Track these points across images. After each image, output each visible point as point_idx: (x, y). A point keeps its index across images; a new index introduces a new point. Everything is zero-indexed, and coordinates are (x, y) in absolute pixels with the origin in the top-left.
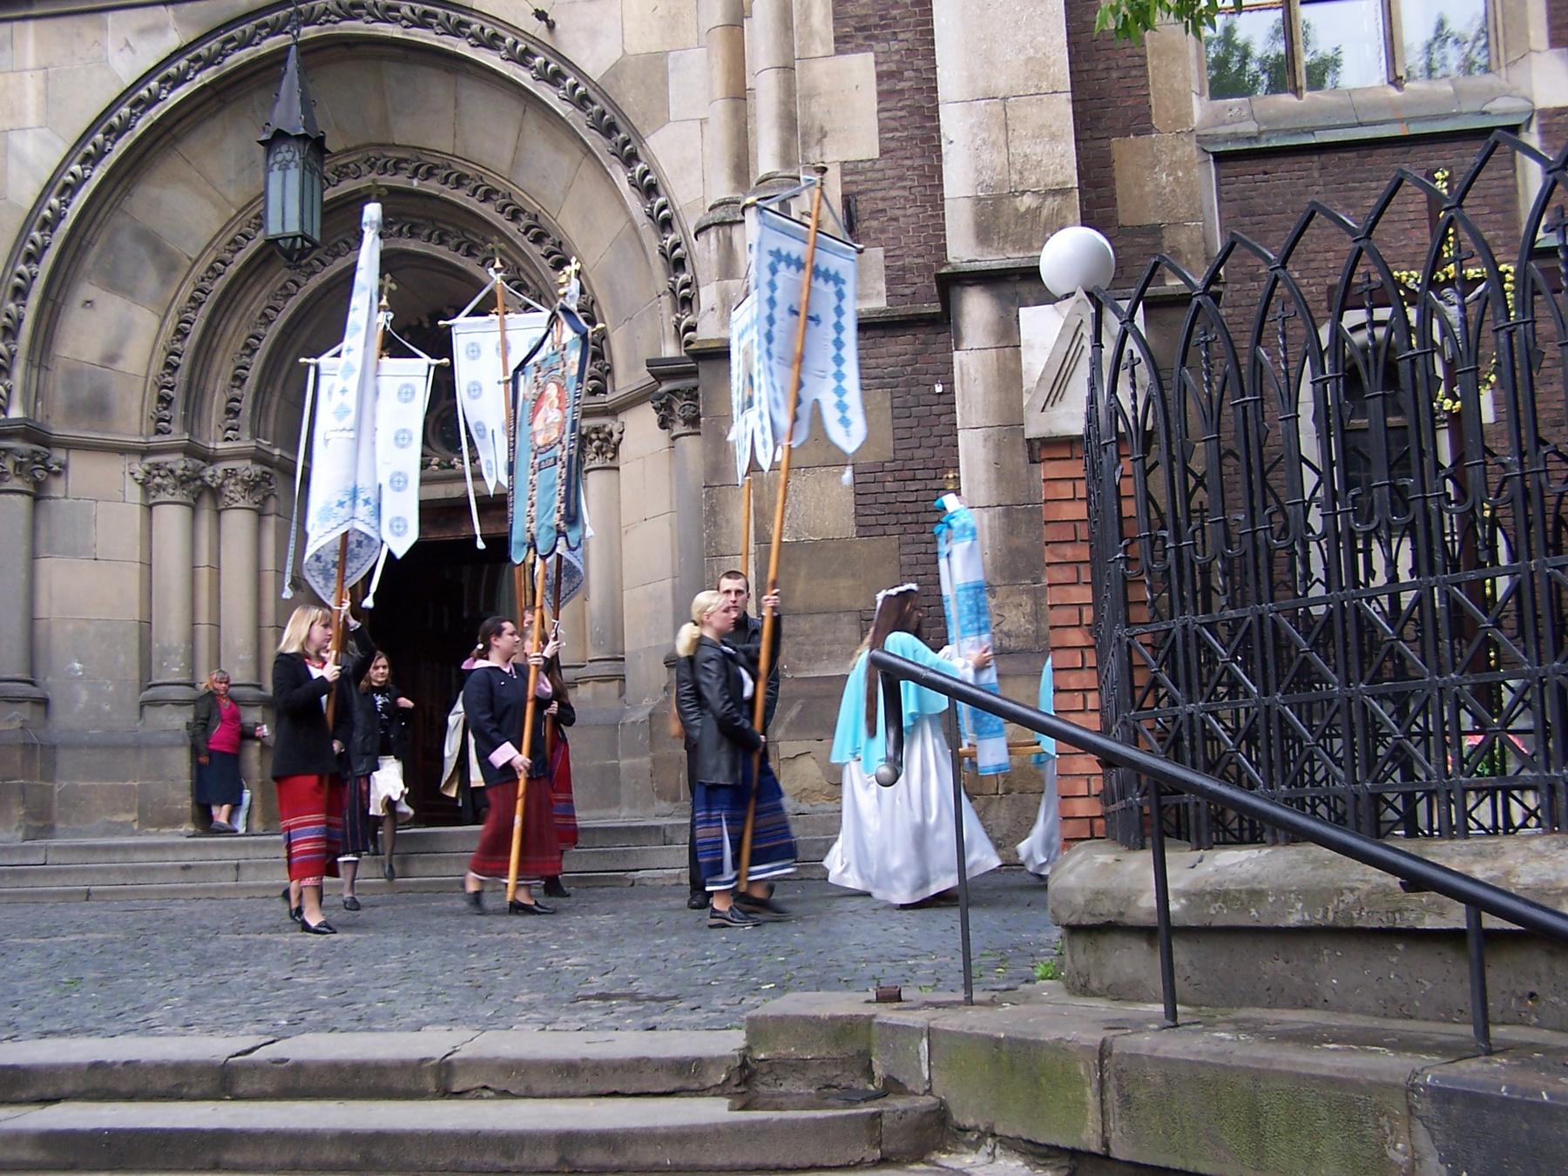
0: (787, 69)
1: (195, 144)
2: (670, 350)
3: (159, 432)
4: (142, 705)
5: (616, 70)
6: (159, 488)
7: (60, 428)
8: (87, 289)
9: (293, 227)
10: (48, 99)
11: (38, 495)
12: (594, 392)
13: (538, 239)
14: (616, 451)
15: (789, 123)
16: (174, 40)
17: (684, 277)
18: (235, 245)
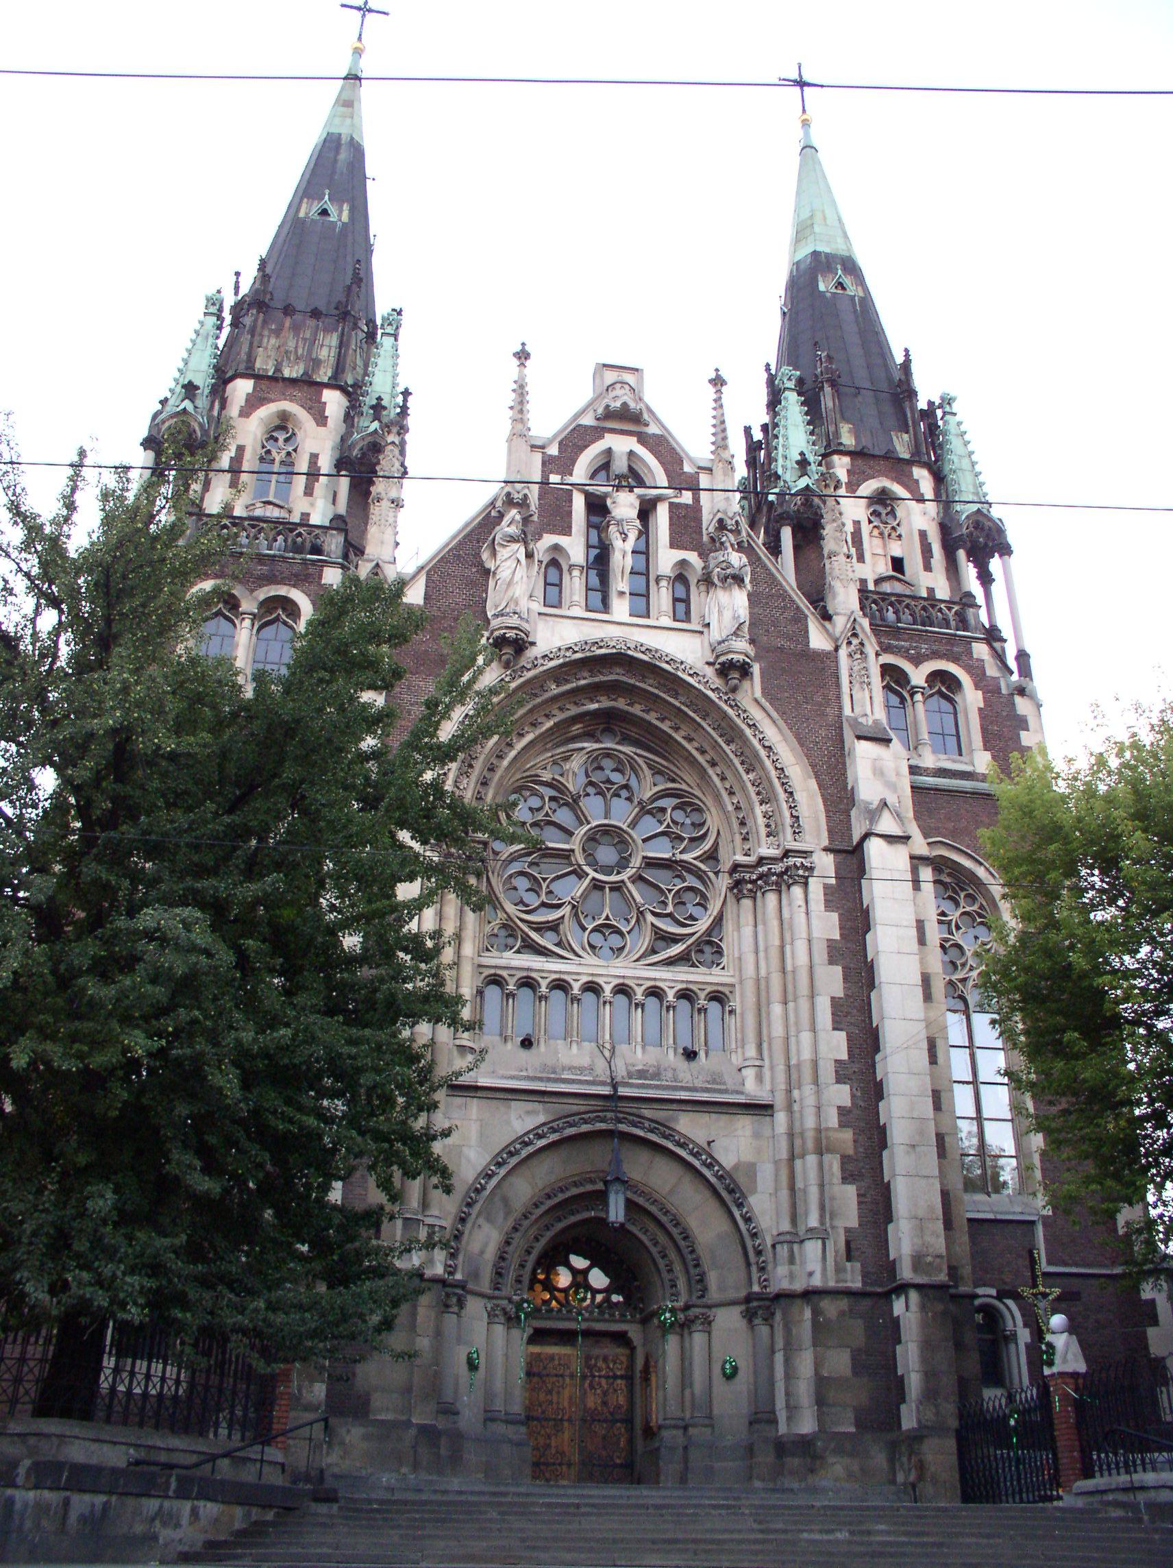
0: (822, 1186)
1: (535, 1161)
2: (756, 1288)
3: (498, 1289)
4: (485, 1420)
5: (737, 1167)
6: (497, 1315)
7: (470, 1286)
8: (481, 1221)
9: (621, 1219)
10: (481, 1135)
11: (458, 1315)
12: (699, 1297)
13: (675, 1226)
14: (710, 1323)
15: (822, 1208)
16: (541, 1119)
17: (762, 1259)
18: (536, 1206)
